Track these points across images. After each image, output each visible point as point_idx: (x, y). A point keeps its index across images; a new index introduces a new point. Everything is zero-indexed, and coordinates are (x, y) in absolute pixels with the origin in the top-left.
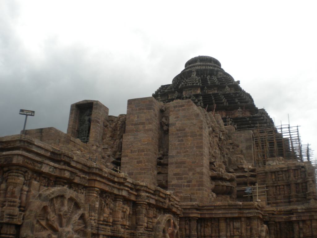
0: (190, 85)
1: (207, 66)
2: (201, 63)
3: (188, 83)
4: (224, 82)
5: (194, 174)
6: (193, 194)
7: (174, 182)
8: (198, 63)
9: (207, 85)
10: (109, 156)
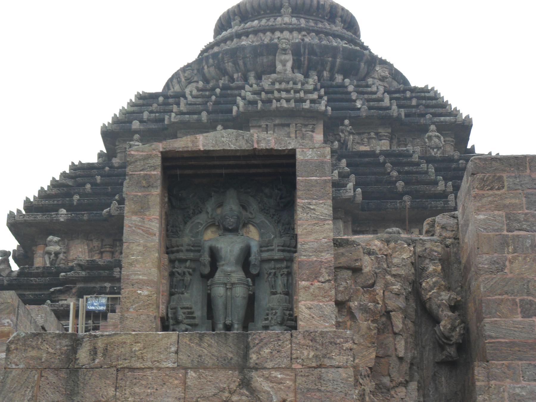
0: (284, 104)
1: (327, 34)
2: (298, 18)
3: (276, 94)
4: (413, 107)
8: (287, 19)
9: (353, 113)
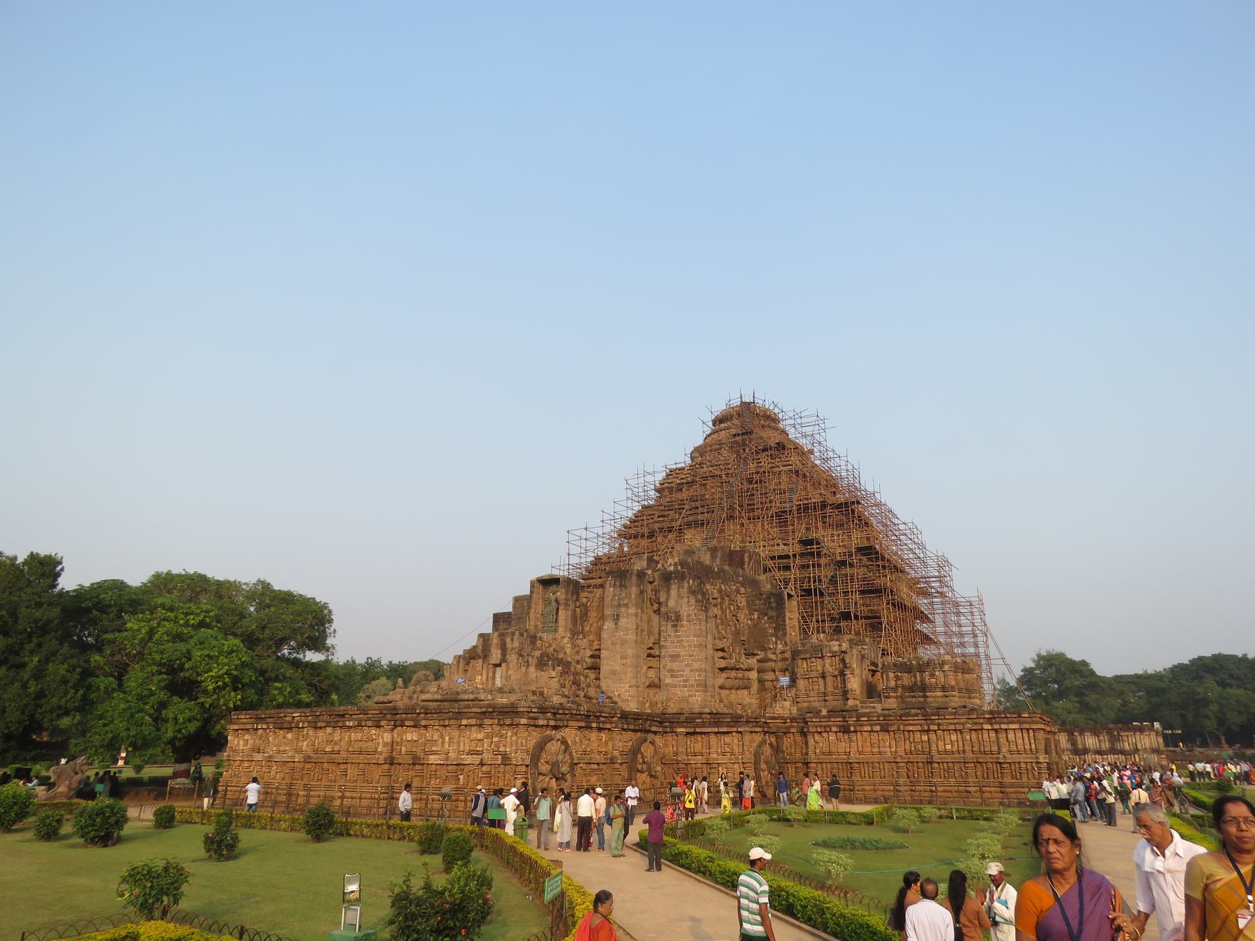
5: (691, 671)
6: (691, 696)
7: (668, 681)
10: (585, 649)
